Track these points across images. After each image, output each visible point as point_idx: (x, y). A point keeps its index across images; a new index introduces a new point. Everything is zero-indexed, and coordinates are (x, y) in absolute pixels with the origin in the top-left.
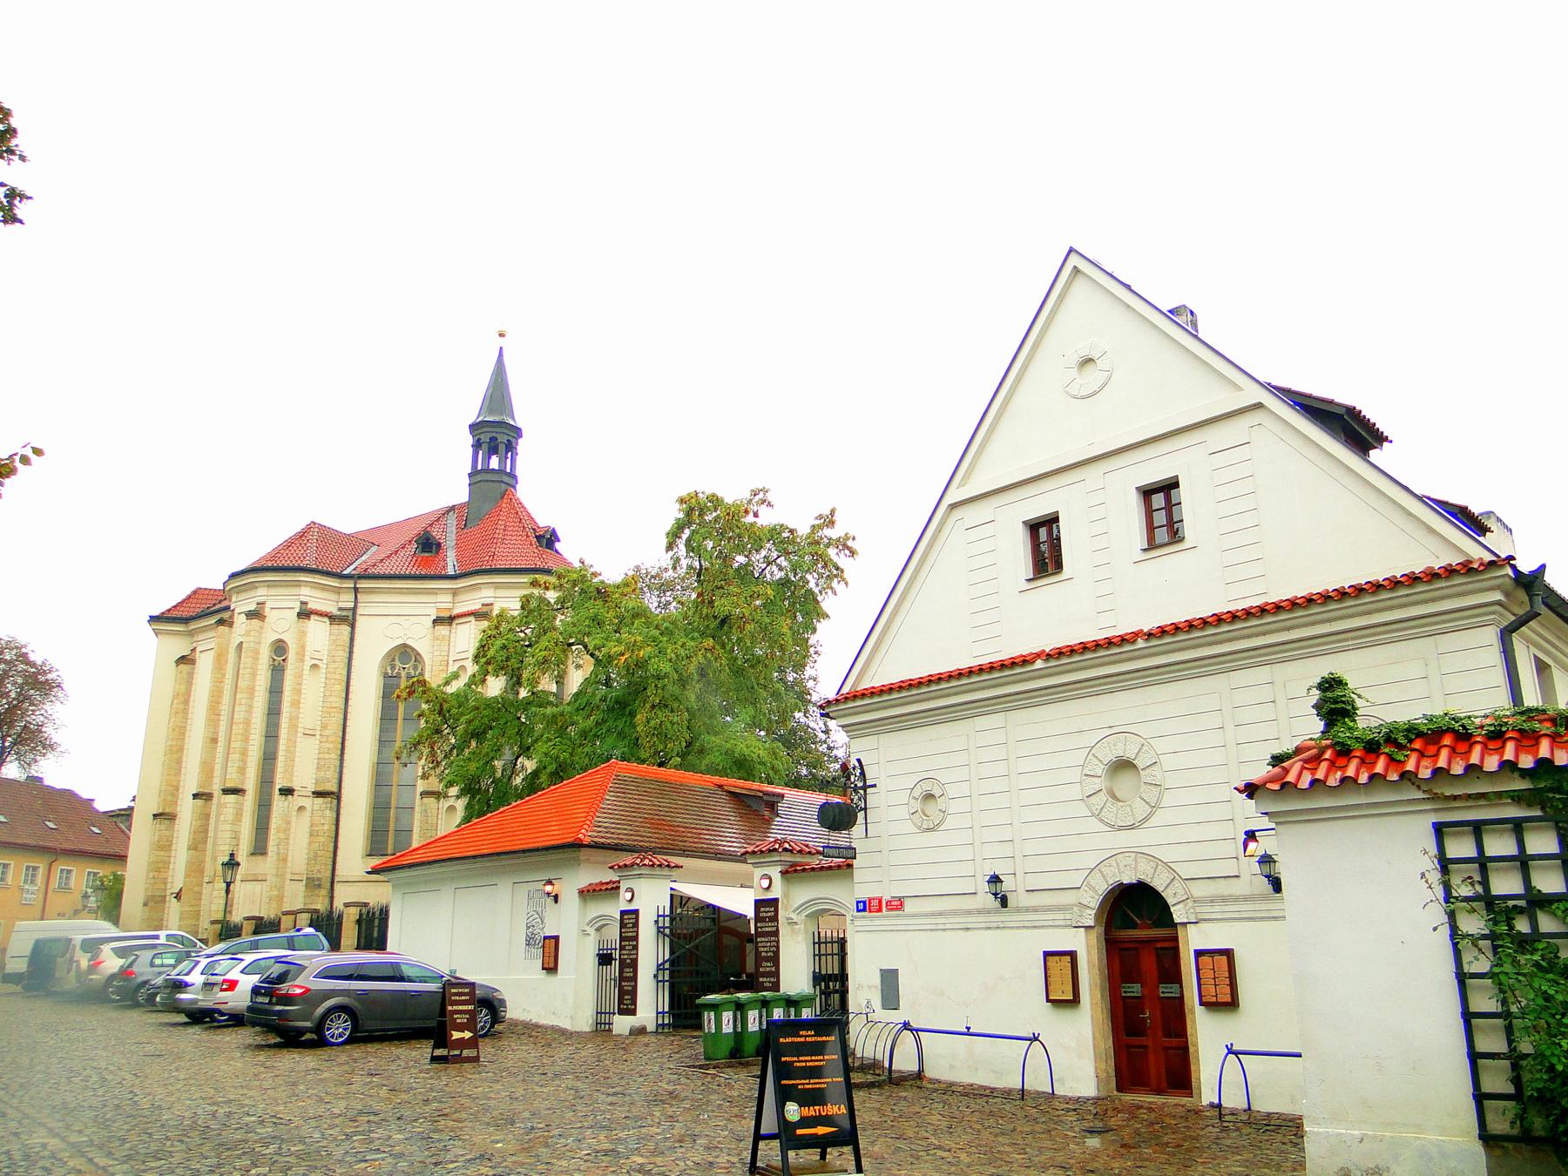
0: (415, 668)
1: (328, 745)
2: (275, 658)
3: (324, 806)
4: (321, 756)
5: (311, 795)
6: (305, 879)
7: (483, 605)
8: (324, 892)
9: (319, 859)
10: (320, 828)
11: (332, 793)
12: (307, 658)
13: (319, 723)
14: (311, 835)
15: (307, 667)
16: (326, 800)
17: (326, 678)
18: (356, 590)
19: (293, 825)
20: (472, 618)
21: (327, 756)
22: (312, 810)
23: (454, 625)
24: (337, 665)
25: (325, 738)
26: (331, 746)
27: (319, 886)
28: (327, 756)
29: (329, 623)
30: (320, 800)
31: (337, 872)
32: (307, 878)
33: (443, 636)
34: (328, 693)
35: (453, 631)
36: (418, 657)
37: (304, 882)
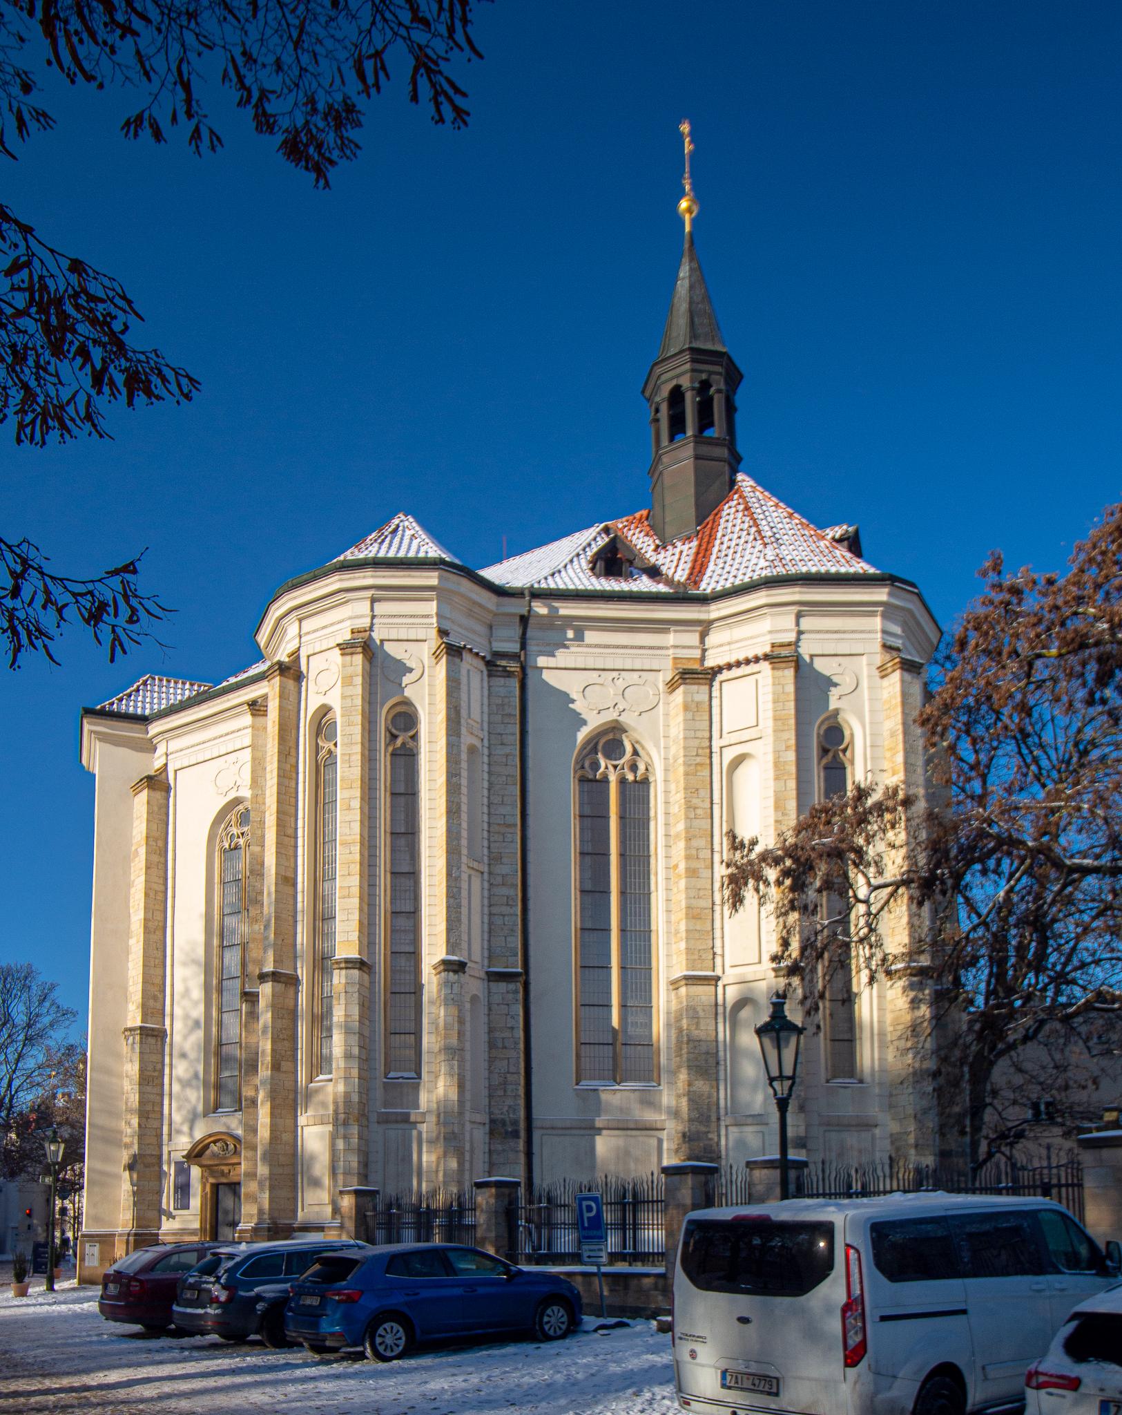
0: (634, 768)
1: (505, 891)
2: (394, 731)
3: (511, 996)
4: (495, 910)
5: (483, 975)
6: (487, 1121)
7: (773, 645)
8: (521, 1145)
9: (510, 1087)
10: (507, 1034)
11: (516, 975)
12: (464, 730)
13: (486, 851)
14: (492, 1045)
15: (464, 748)
16: (512, 986)
17: (490, 773)
18: (524, 620)
19: (468, 1025)
20: (765, 666)
21: (506, 910)
22: (489, 1004)
23: (716, 684)
24: (507, 750)
25: (499, 879)
26: (512, 892)
27: (515, 1134)
28: (506, 910)
29: (485, 673)
30: (502, 986)
31: (536, 1114)
32: (492, 1121)
33: (698, 704)
34: (496, 800)
35: (715, 693)
36: (637, 746)
37: (487, 1127)
